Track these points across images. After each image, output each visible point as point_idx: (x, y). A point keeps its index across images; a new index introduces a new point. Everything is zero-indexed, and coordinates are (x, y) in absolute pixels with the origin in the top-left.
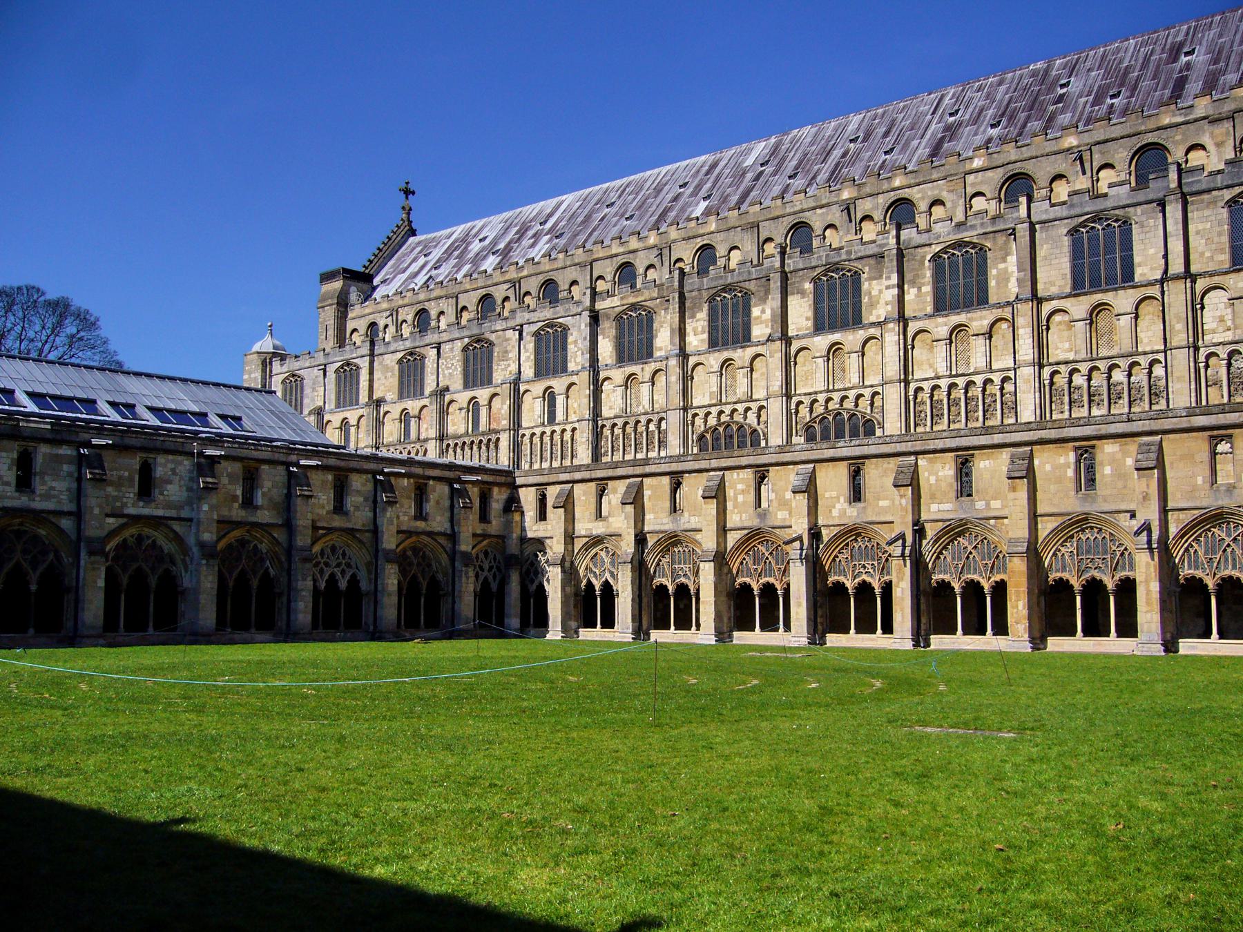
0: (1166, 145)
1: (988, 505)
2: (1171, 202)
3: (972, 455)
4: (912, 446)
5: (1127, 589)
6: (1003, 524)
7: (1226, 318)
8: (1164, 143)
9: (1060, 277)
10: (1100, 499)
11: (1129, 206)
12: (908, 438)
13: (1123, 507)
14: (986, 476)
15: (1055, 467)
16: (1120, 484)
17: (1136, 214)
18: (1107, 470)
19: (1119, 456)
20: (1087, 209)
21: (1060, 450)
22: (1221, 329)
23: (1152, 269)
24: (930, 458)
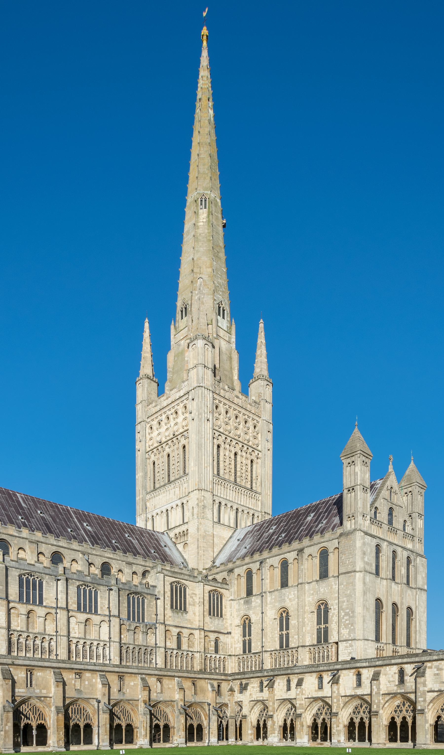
5: (42, 729)
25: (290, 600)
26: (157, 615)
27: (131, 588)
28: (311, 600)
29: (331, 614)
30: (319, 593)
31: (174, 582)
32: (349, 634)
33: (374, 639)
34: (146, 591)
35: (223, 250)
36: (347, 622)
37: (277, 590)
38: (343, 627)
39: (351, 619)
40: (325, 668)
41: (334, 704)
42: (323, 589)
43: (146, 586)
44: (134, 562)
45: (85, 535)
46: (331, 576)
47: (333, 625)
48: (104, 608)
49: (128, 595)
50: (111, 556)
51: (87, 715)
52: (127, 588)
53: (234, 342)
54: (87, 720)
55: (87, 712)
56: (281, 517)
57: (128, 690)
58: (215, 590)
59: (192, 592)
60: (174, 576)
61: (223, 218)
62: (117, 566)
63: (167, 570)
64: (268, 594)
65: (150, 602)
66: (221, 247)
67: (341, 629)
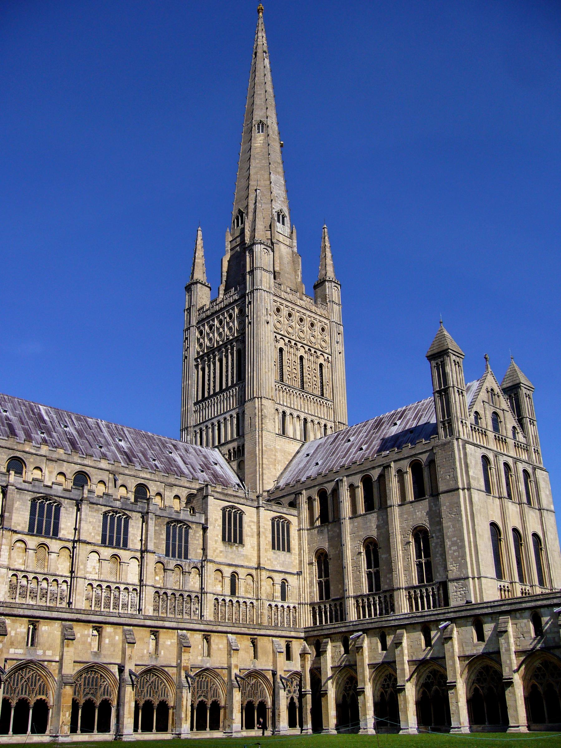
0: (25, 461)
1: (44, 653)
2: (85, 504)
3: (38, 621)
4: (3, 610)
6: (51, 665)
7: (96, 568)
8: (24, 460)
9: (23, 522)
10: (102, 656)
11: (62, 497)
12: (68, 610)
13: (112, 661)
14: (46, 635)
15: (82, 635)
16: (112, 649)
17: (65, 502)
18: (107, 641)
19: (113, 634)
20: (41, 491)
21: (86, 627)
22: (93, 573)
23: (68, 533)
24: (13, 619)
26: (204, 549)
27: (172, 515)
28: (406, 527)
29: (433, 544)
31: (227, 507)
33: (494, 576)
34: (190, 518)
35: (281, 165)
37: (361, 515)
38: (451, 560)
43: (190, 512)
44: (177, 483)
45: (116, 452)
47: (437, 558)
48: (135, 541)
49: (168, 523)
50: (148, 476)
51: (104, 688)
52: (165, 514)
53: (295, 246)
54: (104, 694)
55: (105, 683)
56: (360, 426)
57: (162, 652)
58: (280, 517)
59: (250, 519)
60: (227, 499)
61: (280, 140)
62: (155, 489)
63: (217, 492)
65: (196, 532)
66: (279, 163)
67: (448, 563)
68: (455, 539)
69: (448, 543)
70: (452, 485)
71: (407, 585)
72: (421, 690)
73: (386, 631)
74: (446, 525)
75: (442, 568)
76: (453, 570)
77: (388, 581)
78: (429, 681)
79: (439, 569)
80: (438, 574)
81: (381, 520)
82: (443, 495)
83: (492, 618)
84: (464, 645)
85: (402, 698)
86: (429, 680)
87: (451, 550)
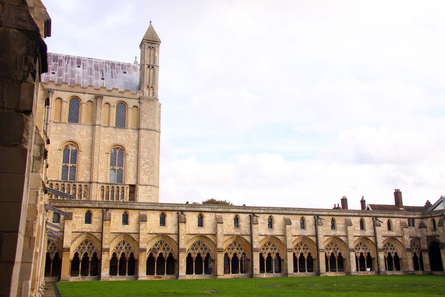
25: (82, 136)
28: (107, 143)
29: (128, 160)
30: (116, 138)
32: (149, 179)
36: (147, 170)
37: (66, 123)
38: (143, 173)
39: (151, 168)
40: (170, 208)
41: (182, 241)
42: (120, 136)
46: (129, 127)
47: (129, 169)
64: (53, 124)
67: (141, 174)
68: (148, 160)
69: (142, 162)
70: (151, 126)
71: (101, 182)
72: (149, 253)
73: (130, 212)
74: (143, 150)
75: (133, 176)
76: (144, 178)
77: (85, 175)
78: (156, 248)
79: (130, 176)
80: (128, 180)
81: (84, 132)
82: (143, 130)
83: (210, 214)
84: (190, 227)
85: (143, 257)
86: (156, 246)
87: (144, 166)
